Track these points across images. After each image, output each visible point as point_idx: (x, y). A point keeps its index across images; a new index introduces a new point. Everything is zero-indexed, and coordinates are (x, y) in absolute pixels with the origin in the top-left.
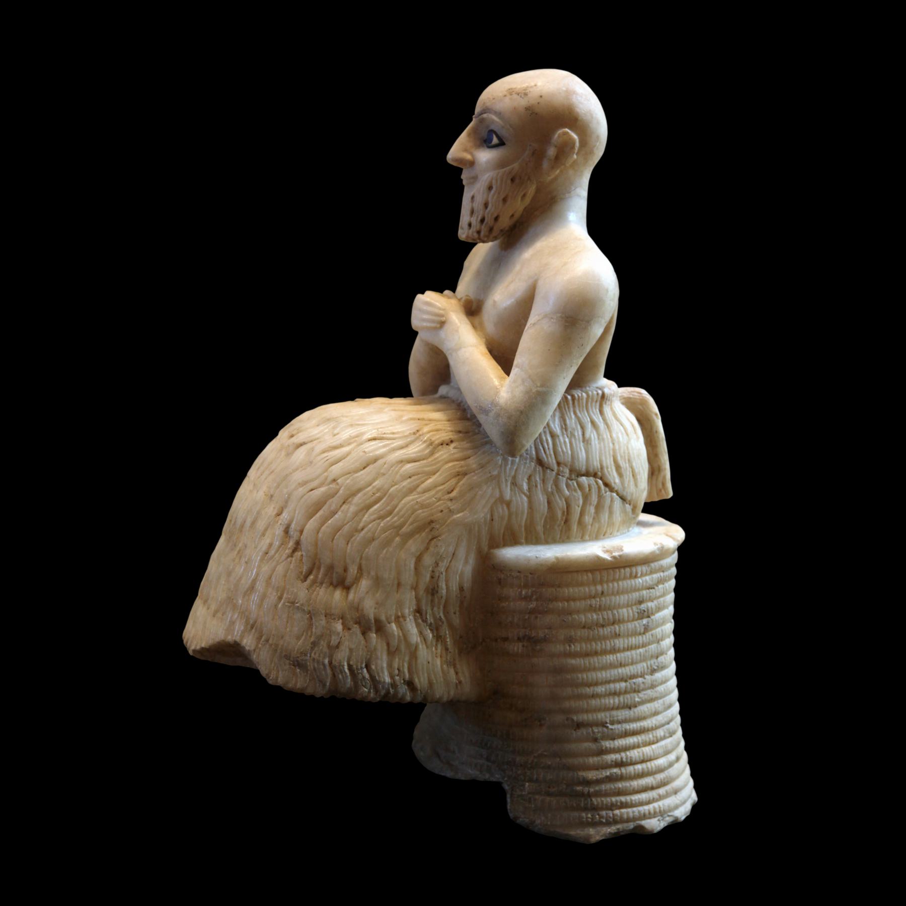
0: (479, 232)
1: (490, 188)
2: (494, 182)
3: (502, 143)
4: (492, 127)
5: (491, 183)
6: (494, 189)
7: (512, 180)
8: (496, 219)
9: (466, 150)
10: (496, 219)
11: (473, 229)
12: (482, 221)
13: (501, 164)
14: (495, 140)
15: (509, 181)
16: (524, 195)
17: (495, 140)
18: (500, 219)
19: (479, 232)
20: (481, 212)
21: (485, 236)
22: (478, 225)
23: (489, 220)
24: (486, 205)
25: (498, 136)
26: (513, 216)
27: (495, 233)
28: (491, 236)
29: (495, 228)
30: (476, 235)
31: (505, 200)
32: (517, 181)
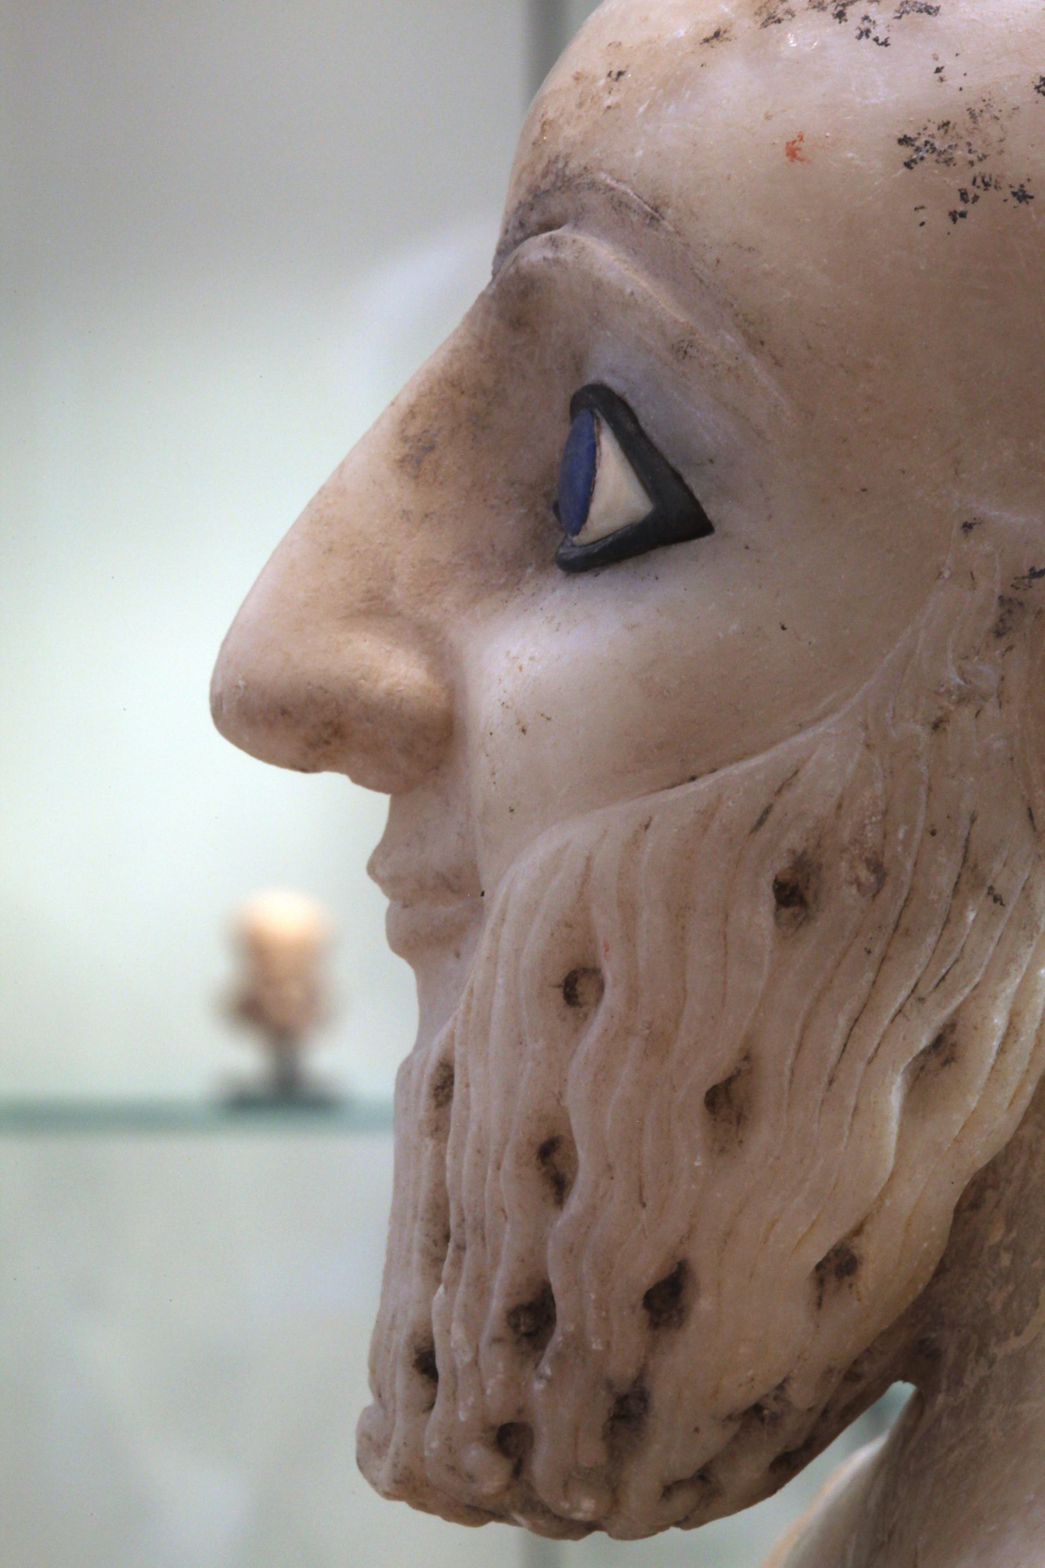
0: (510, 1438)
1: (575, 986)
2: (605, 923)
3: (675, 522)
4: (610, 365)
5: (575, 925)
6: (613, 997)
7: (792, 895)
8: (667, 1299)
9: (374, 608)
10: (667, 1299)
11: (460, 1408)
12: (533, 1318)
13: (672, 737)
14: (617, 493)
15: (760, 914)
16: (944, 1050)
17: (617, 493)
18: (703, 1305)
19: (510, 1438)
20: (510, 1242)
21: (571, 1478)
22: (496, 1364)
23: (597, 1318)
24: (551, 1160)
25: (639, 449)
26: (840, 1266)
27: (670, 1447)
28: (643, 1479)
29: (662, 1393)
30: (489, 1473)
31: (727, 1103)
32: (842, 896)
